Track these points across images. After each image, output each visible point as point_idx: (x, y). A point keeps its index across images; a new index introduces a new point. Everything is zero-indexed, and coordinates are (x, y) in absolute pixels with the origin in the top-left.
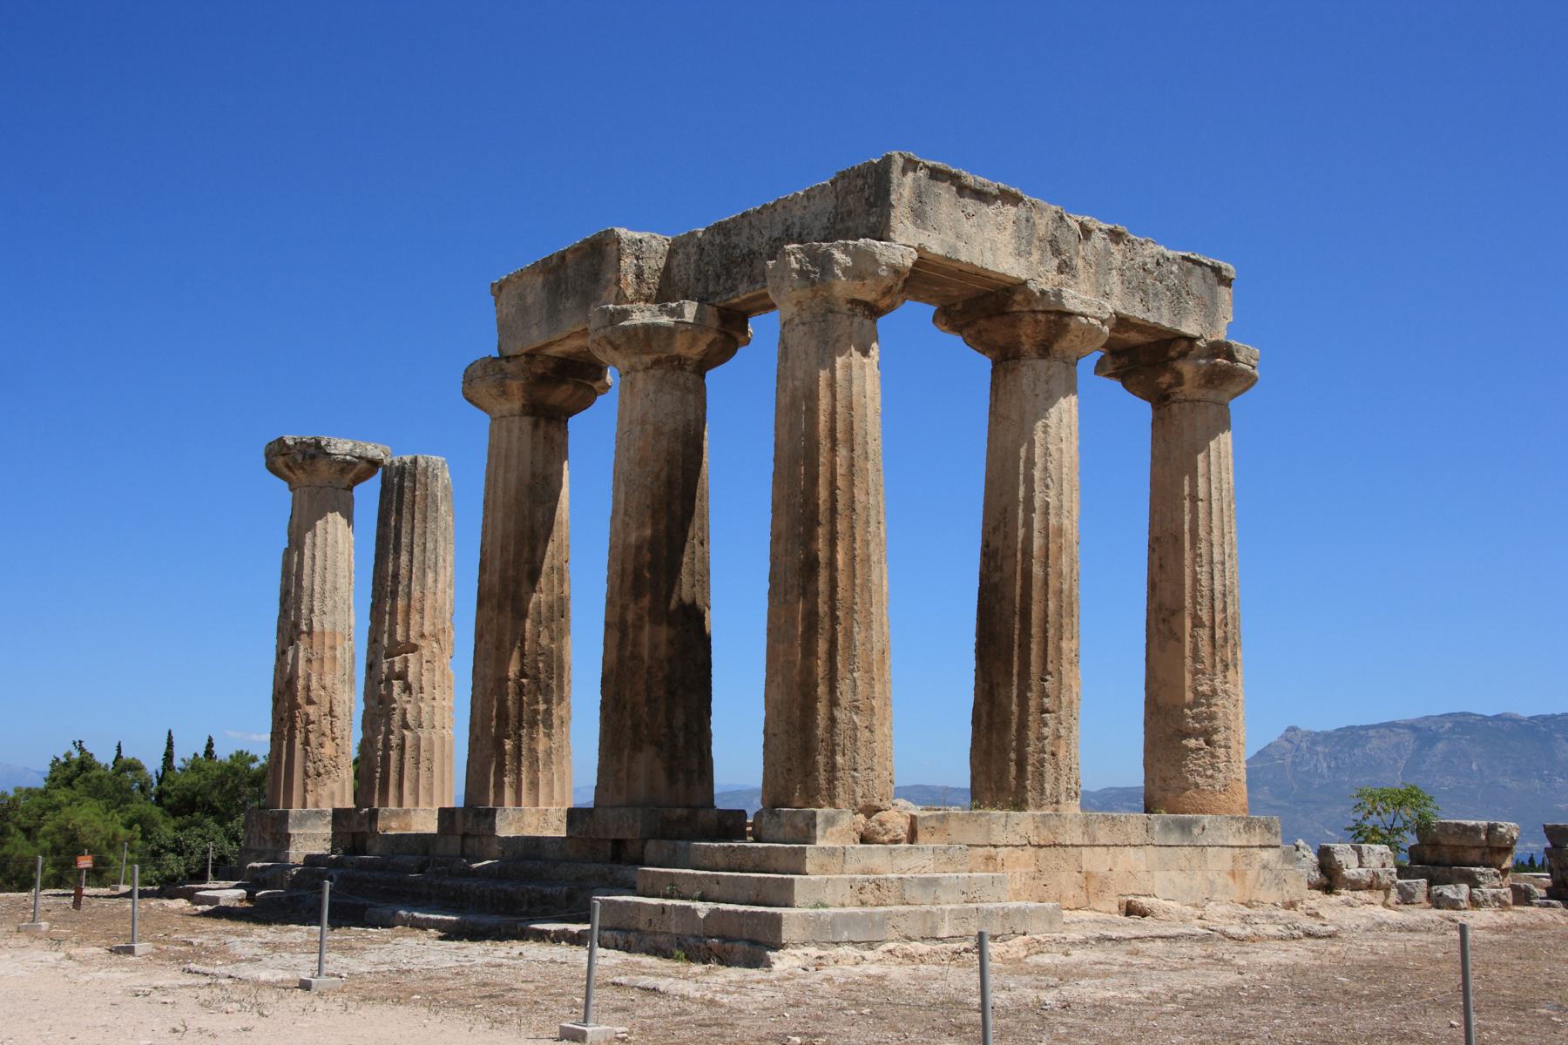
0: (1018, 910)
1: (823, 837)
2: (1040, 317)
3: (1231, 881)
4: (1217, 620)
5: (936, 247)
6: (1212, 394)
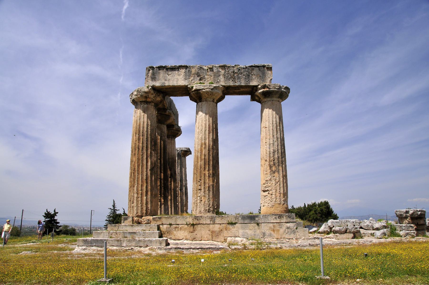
0: (149, 240)
1: (123, 222)
2: (194, 92)
3: (272, 232)
4: (271, 160)
5: (157, 84)
6: (269, 99)
